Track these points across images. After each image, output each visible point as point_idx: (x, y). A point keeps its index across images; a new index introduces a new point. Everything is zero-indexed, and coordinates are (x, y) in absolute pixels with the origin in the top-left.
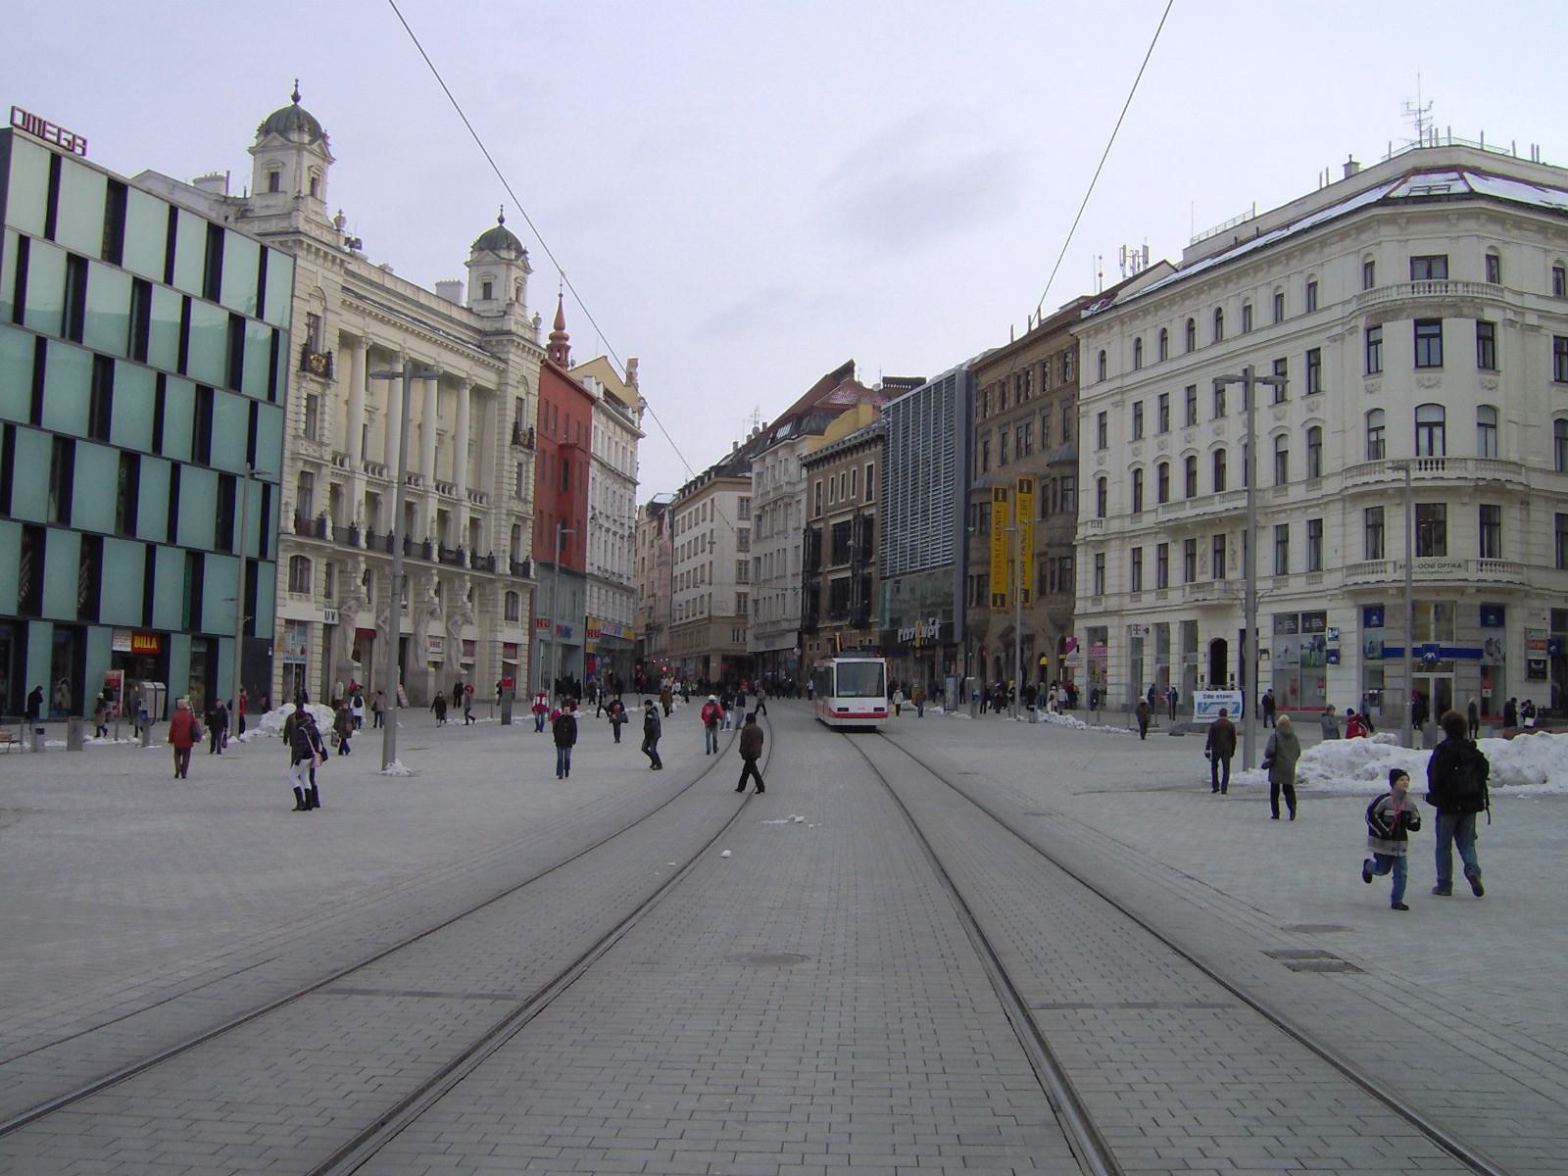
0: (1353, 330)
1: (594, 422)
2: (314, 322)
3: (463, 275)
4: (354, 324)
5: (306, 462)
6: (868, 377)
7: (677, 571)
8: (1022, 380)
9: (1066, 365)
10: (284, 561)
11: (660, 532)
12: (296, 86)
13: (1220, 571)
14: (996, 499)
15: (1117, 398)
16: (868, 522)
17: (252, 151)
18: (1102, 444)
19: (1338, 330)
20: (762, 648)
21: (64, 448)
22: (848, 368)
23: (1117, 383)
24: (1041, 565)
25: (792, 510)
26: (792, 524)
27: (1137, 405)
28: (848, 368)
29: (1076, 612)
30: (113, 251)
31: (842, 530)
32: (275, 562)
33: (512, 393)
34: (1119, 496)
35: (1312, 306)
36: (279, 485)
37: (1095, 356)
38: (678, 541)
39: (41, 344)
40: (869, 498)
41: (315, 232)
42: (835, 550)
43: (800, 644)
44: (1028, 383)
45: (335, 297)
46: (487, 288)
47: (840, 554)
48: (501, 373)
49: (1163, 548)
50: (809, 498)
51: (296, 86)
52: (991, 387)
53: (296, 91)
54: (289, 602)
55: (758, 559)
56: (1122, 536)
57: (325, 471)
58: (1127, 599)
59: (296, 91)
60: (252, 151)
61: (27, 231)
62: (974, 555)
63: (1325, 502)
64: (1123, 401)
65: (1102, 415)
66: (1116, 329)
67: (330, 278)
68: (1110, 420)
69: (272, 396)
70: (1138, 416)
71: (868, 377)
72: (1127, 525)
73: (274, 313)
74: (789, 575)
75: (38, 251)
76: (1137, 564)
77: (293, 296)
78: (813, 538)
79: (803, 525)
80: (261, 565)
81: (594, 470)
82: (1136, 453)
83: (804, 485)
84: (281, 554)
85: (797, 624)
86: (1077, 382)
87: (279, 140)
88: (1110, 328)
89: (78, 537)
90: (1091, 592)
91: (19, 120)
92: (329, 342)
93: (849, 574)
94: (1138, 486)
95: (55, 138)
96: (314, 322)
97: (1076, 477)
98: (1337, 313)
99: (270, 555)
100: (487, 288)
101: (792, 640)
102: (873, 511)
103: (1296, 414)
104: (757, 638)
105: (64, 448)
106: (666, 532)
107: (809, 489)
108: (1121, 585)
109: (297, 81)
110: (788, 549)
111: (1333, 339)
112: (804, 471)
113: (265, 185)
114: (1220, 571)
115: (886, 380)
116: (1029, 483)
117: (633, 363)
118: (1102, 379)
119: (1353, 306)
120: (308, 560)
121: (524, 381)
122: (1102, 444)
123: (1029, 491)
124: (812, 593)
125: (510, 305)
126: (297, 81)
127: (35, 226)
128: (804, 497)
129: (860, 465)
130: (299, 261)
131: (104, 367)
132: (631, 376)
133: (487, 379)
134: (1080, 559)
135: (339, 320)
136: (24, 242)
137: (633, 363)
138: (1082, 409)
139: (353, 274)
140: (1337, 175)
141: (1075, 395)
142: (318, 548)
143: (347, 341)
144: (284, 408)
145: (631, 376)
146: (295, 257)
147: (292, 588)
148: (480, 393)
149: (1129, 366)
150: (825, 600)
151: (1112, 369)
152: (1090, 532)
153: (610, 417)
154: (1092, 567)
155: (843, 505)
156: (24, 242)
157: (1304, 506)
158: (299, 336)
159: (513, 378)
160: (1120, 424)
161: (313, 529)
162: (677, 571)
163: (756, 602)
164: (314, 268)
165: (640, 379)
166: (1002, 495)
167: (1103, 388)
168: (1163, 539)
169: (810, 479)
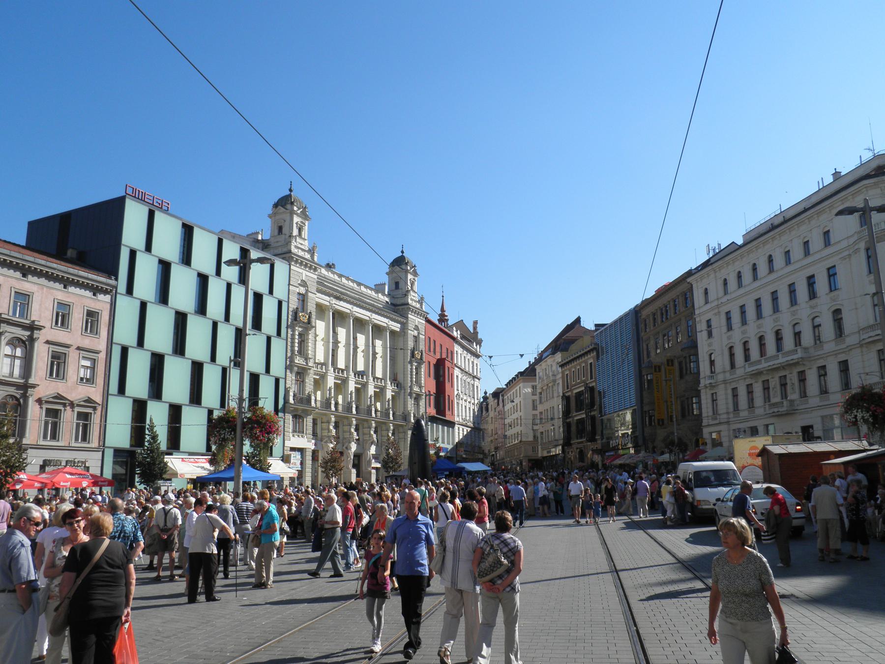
0: (857, 251)
1: (456, 349)
2: (303, 298)
3: (385, 279)
4: (324, 300)
6: (588, 324)
7: (507, 421)
8: (664, 311)
9: (686, 299)
11: (498, 404)
13: (784, 395)
14: (655, 371)
15: (716, 311)
16: (592, 389)
17: (270, 216)
18: (710, 334)
19: (846, 253)
20: (545, 454)
21: (157, 361)
22: (578, 320)
23: (716, 303)
24: (682, 402)
25: (555, 388)
26: (555, 395)
27: (728, 313)
28: (578, 320)
29: (703, 424)
30: (186, 259)
31: (580, 394)
33: (412, 333)
34: (722, 362)
35: (827, 243)
37: (702, 291)
38: (506, 408)
39: (143, 305)
40: (591, 378)
41: (301, 253)
42: (577, 406)
43: (563, 451)
44: (667, 311)
45: (313, 287)
46: (397, 285)
47: (579, 408)
48: (404, 326)
49: (749, 386)
50: (563, 382)
52: (648, 316)
54: (292, 438)
55: (541, 413)
56: (725, 382)
57: (312, 372)
58: (731, 415)
60: (270, 216)
61: (135, 246)
62: (646, 401)
63: (850, 349)
64: (719, 312)
65: (709, 321)
66: (712, 276)
68: (713, 324)
69: (279, 333)
70: (729, 319)
71: (588, 324)
72: (728, 376)
73: (280, 290)
74: (556, 417)
75: (141, 258)
76: (735, 395)
77: (289, 284)
78: (566, 399)
79: (561, 394)
81: (457, 372)
82: (729, 338)
83: (560, 375)
85: (561, 442)
86: (693, 306)
87: (282, 209)
88: (708, 275)
90: (711, 413)
91: (129, 191)
92: (311, 307)
93: (584, 416)
94: (732, 355)
95: (151, 202)
96: (303, 298)
97: (696, 355)
98: (844, 244)
100: (397, 285)
101: (558, 450)
102: (594, 384)
103: (825, 303)
104: (543, 449)
105: (157, 361)
106: (501, 404)
107: (563, 377)
108: (727, 408)
110: (557, 405)
111: (844, 258)
112: (560, 369)
113: (276, 231)
114: (784, 395)
115: (596, 325)
116: (672, 361)
117: (475, 323)
118: (707, 302)
119: (856, 237)
121: (417, 328)
122: (710, 334)
123: (672, 365)
124: (567, 426)
125: (408, 291)
127: (140, 245)
128: (560, 382)
129: (586, 362)
131: (181, 319)
132: (475, 328)
133: (396, 327)
134: (703, 397)
135: (316, 298)
136: (133, 254)
137: (475, 323)
138: (697, 320)
140: (829, 179)
141: (693, 313)
143: (321, 309)
145: (475, 328)
146: (290, 265)
147: (294, 431)
148: (393, 333)
149: (721, 293)
150: (573, 428)
151: (712, 296)
152: (708, 382)
153: (463, 347)
154: (710, 401)
155: (579, 383)
156: (133, 254)
157: (836, 354)
158: (294, 303)
159: (411, 326)
160: (719, 324)
162: (507, 421)
163: (542, 433)
164: (301, 271)
165: (478, 330)
166: (658, 368)
167: (708, 306)
168: (749, 381)
169: (563, 373)
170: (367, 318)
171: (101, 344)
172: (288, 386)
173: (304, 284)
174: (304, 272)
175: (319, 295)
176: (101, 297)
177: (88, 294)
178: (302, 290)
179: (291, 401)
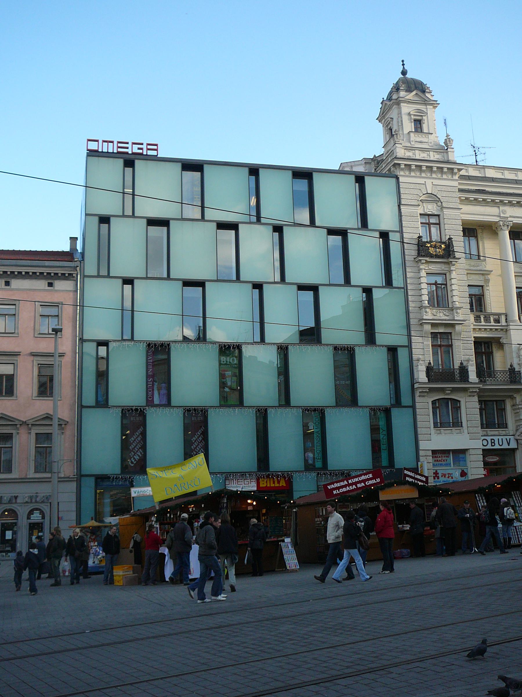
5: (433, 325)
10: (424, 406)
12: (403, 65)
32: (413, 407)
36: (409, 347)
51: (403, 65)
53: (404, 67)
59: (404, 67)
67: (447, 186)
80: (395, 412)
84: (417, 399)
89: (180, 413)
99: (406, 400)
109: (403, 61)
120: (459, 401)
126: (403, 61)
130: (401, 179)
139: (462, 177)
142: (465, 390)
144: (405, 289)
161: (457, 376)
164: (422, 181)
170: (496, 219)
171: (66, 344)
172: (415, 357)
173: (433, 198)
174: (429, 182)
175: (466, 208)
176: (59, 285)
177: (42, 284)
178: (431, 208)
179: (422, 376)
